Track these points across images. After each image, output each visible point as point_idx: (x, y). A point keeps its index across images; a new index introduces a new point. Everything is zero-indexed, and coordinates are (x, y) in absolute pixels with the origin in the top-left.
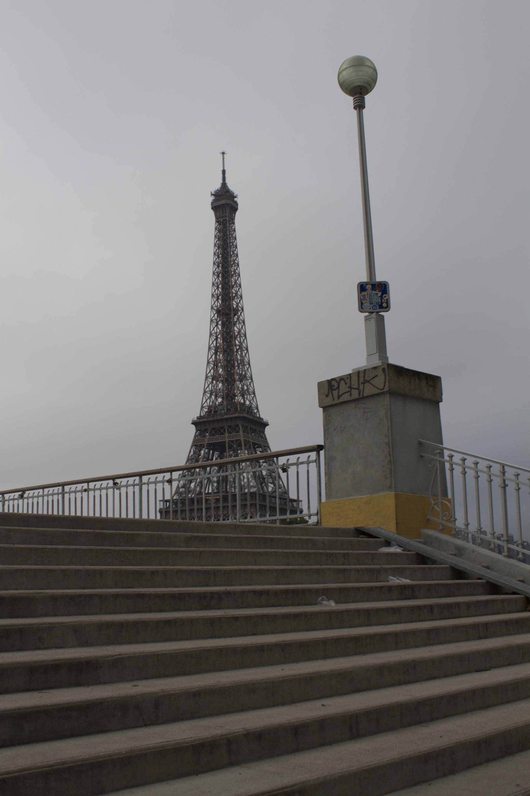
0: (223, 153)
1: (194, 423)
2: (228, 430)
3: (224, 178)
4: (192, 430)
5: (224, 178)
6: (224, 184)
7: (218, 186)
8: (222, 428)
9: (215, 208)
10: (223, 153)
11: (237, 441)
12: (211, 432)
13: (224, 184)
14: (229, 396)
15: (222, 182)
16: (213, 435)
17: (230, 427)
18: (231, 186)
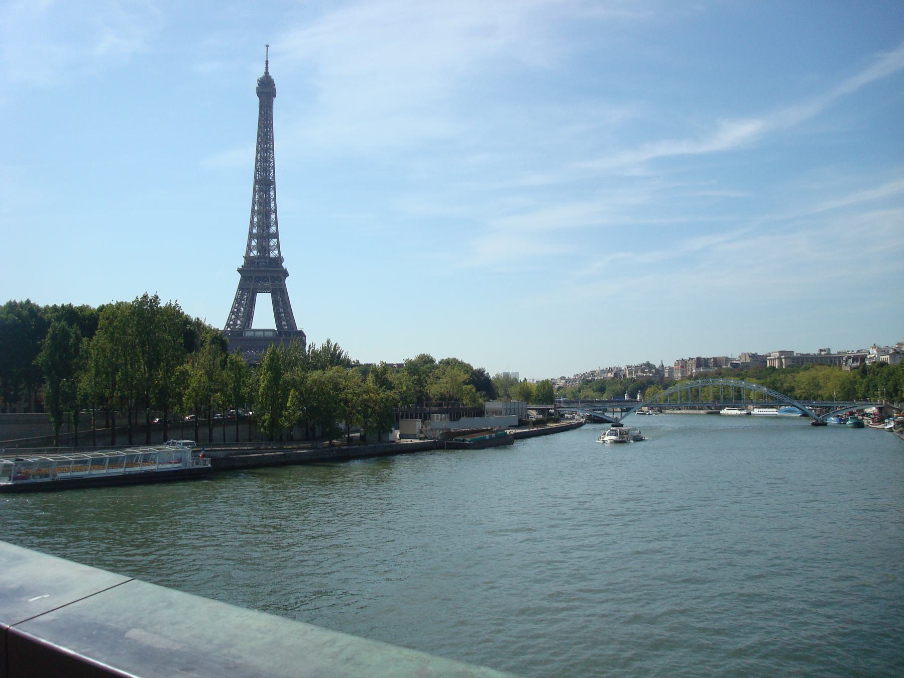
0: (267, 46)
1: (239, 271)
2: (271, 280)
3: (267, 68)
4: (238, 276)
5: (267, 68)
6: (267, 73)
7: (261, 74)
8: (266, 277)
9: (259, 94)
10: (267, 46)
11: (279, 289)
12: (255, 279)
13: (267, 73)
14: (264, 249)
15: (265, 71)
16: (257, 282)
17: (272, 277)
18: (271, 73)
